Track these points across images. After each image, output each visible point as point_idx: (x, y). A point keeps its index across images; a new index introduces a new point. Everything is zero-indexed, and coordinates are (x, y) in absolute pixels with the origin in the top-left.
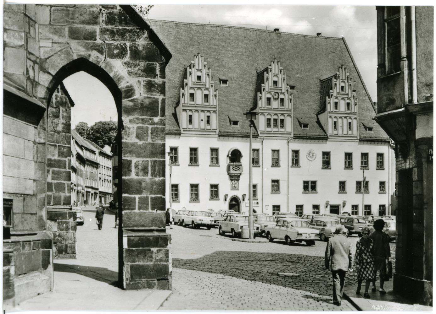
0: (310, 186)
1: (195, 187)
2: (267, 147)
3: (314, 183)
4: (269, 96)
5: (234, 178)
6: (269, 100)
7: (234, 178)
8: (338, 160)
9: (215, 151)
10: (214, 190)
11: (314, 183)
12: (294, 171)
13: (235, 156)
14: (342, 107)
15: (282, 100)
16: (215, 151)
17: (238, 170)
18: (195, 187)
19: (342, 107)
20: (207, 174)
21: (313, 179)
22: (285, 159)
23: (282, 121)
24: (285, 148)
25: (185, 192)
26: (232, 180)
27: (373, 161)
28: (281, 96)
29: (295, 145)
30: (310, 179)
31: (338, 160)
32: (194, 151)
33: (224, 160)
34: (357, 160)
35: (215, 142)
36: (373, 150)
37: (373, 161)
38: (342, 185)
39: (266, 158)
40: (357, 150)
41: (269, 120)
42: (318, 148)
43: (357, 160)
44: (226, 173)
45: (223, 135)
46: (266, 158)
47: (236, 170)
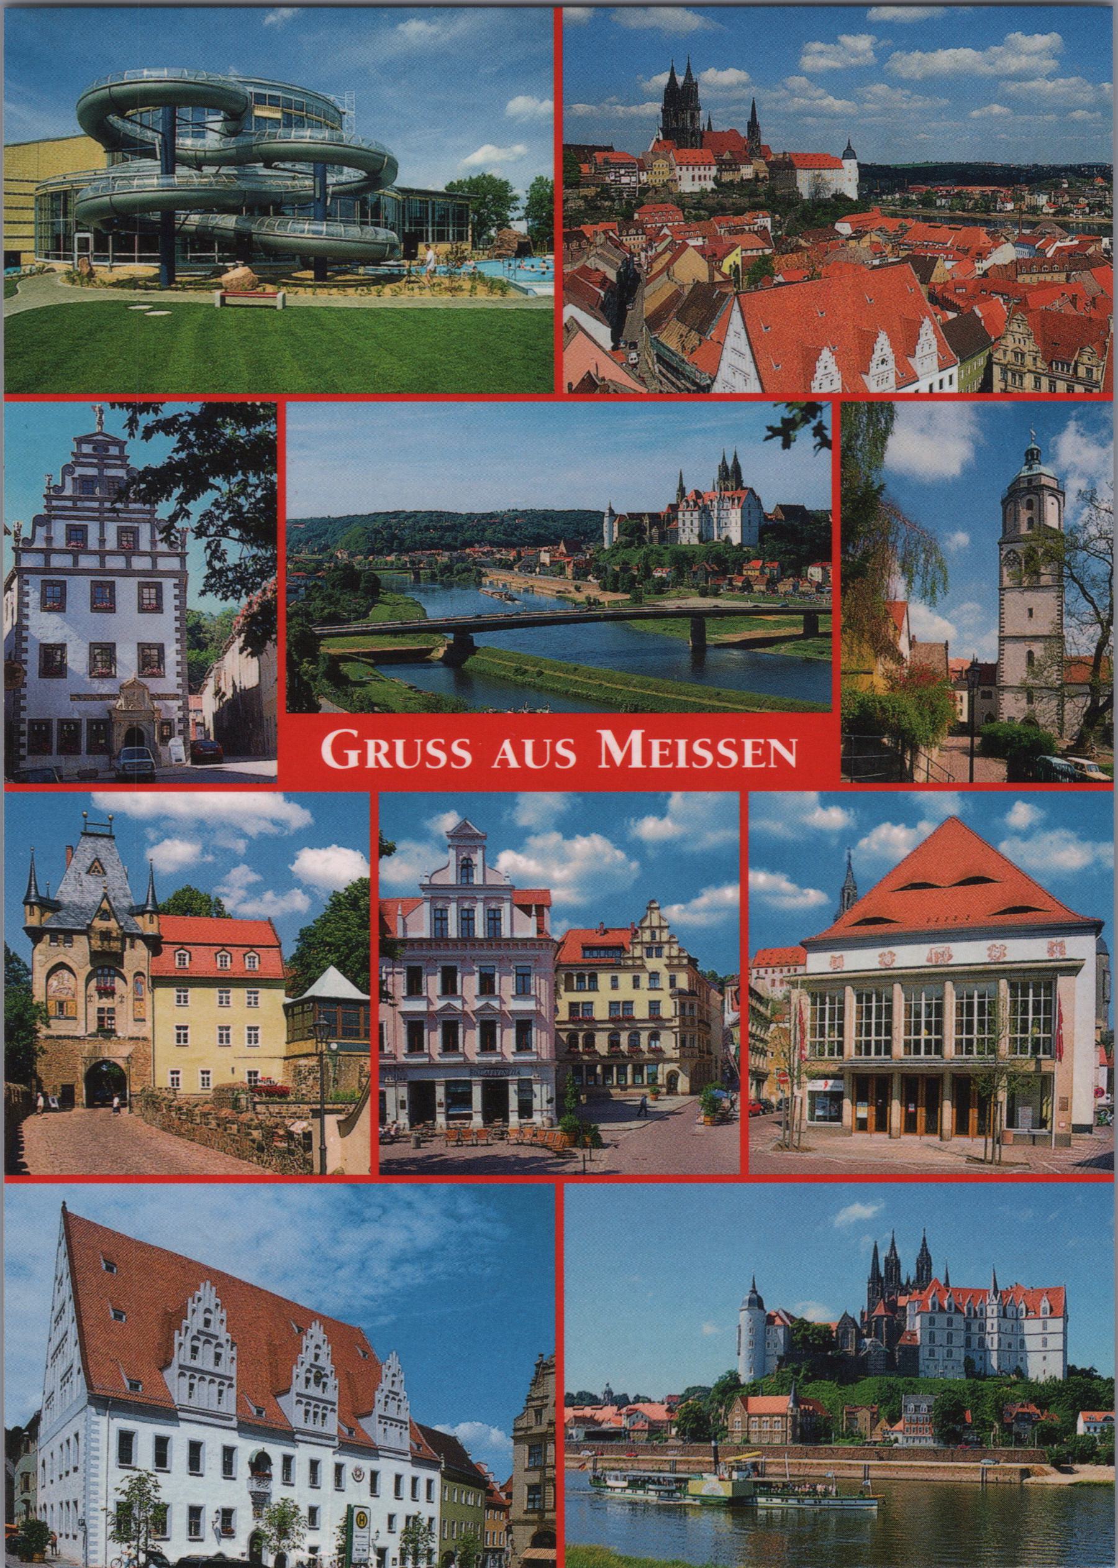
1: (195, 1512)
9: (228, 1452)
15: (325, 1384)
16: (228, 1452)
18: (195, 1512)
20: (216, 1492)
22: (327, 1474)
23: (324, 1416)
25: (178, 1521)
29: (339, 1459)
32: (195, 1448)
35: (232, 1438)
39: (301, 1471)
41: (307, 1412)
42: (367, 1465)
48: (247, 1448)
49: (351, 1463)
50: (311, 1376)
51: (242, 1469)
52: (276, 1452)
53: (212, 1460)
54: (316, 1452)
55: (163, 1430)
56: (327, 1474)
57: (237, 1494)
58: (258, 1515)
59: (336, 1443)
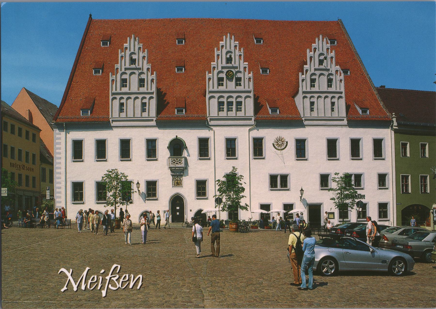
0: (279, 182)
2: (218, 137)
3: (284, 179)
4: (221, 75)
5: (178, 174)
6: (220, 80)
7: (178, 174)
8: (316, 147)
10: (151, 189)
11: (284, 179)
12: (257, 163)
13: (177, 147)
14: (322, 84)
15: (239, 80)
17: (180, 162)
19: (322, 84)
21: (284, 172)
22: (244, 148)
23: (239, 104)
24: (244, 137)
26: (172, 175)
27: (367, 148)
28: (239, 75)
30: (279, 171)
31: (316, 147)
33: (163, 151)
34: (344, 148)
36: (367, 136)
37: (367, 148)
38: (324, 180)
39: (218, 148)
40: (344, 135)
41: (221, 104)
43: (344, 148)
44: (167, 167)
45: (162, 124)
46: (218, 148)
47: (177, 164)
48: (164, 137)
49: (269, 135)
50: (223, 75)
51: (163, 151)
52: (190, 137)
53: (138, 150)
54: (231, 132)
55: (101, 134)
56: (244, 148)
57: (160, 170)
58: (177, 183)
59: (252, 122)
